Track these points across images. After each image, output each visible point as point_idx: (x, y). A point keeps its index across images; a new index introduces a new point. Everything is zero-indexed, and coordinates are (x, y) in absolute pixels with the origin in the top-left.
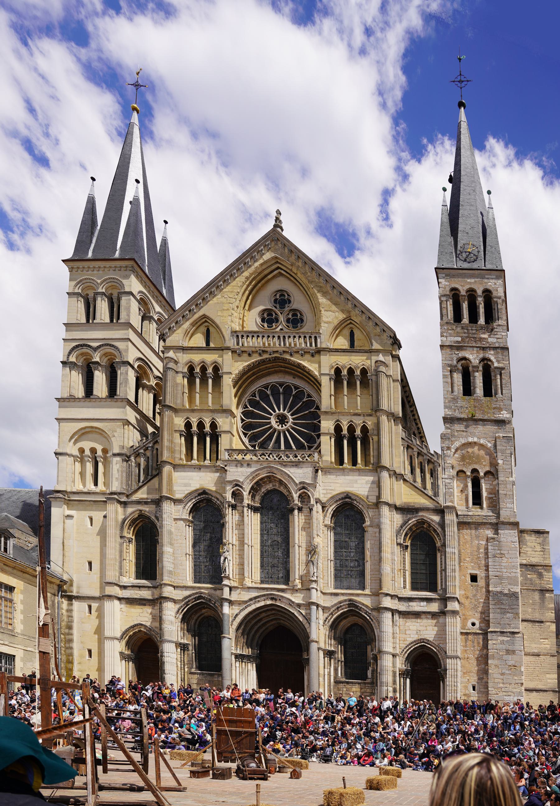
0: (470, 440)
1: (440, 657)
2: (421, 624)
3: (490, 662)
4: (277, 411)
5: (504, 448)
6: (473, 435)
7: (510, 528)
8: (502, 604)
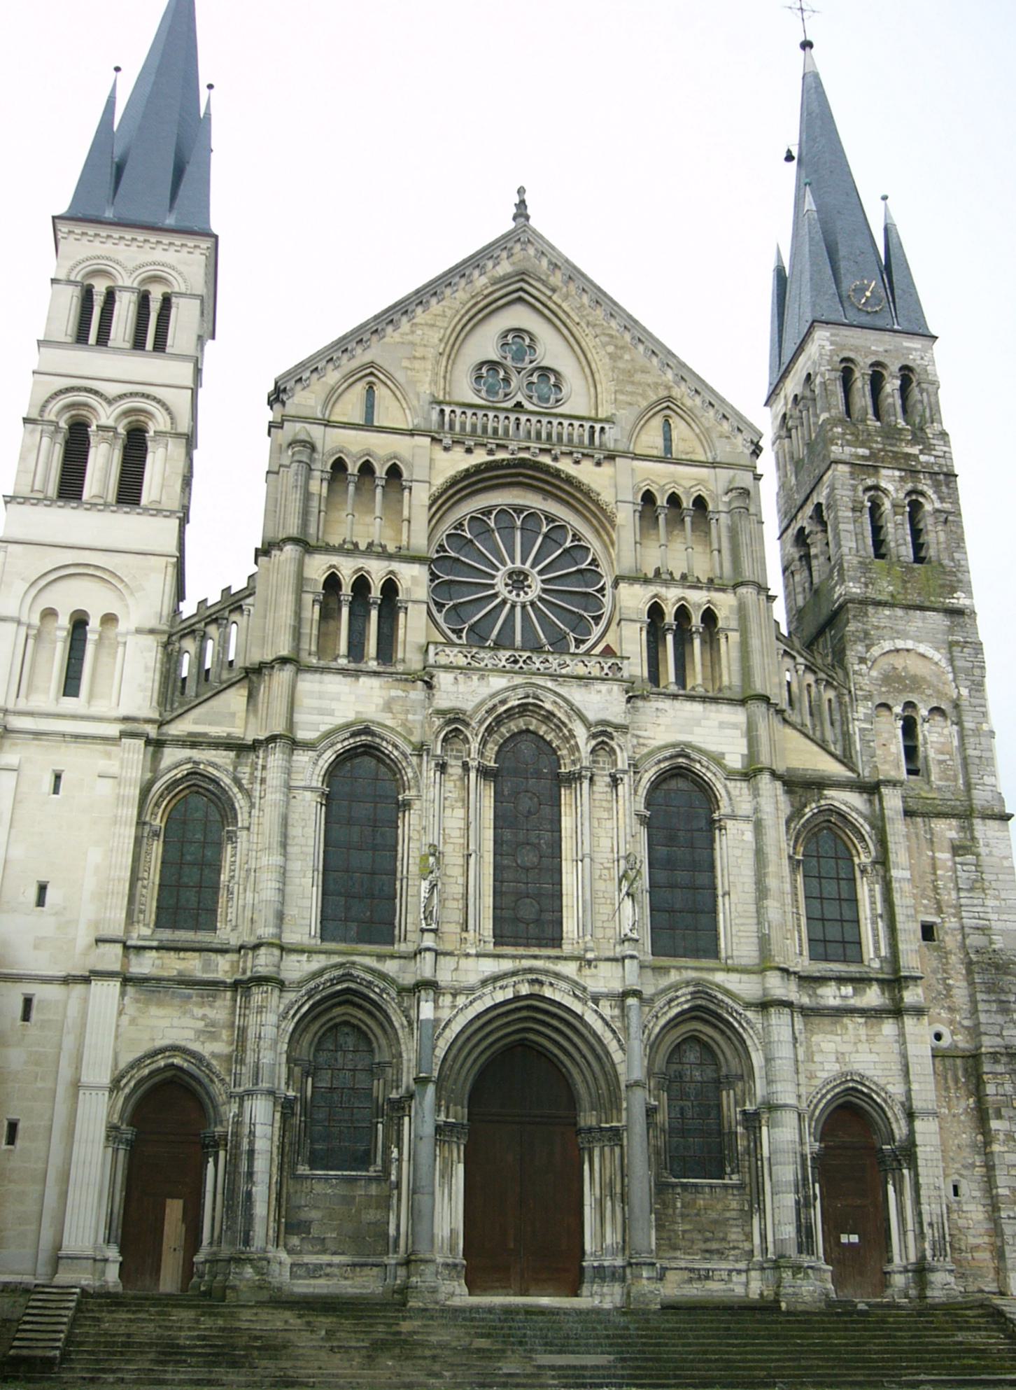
0: (900, 644)
1: (890, 1114)
2: (846, 1038)
3: (994, 1124)
5: (970, 665)
6: (903, 635)
8: (1002, 991)
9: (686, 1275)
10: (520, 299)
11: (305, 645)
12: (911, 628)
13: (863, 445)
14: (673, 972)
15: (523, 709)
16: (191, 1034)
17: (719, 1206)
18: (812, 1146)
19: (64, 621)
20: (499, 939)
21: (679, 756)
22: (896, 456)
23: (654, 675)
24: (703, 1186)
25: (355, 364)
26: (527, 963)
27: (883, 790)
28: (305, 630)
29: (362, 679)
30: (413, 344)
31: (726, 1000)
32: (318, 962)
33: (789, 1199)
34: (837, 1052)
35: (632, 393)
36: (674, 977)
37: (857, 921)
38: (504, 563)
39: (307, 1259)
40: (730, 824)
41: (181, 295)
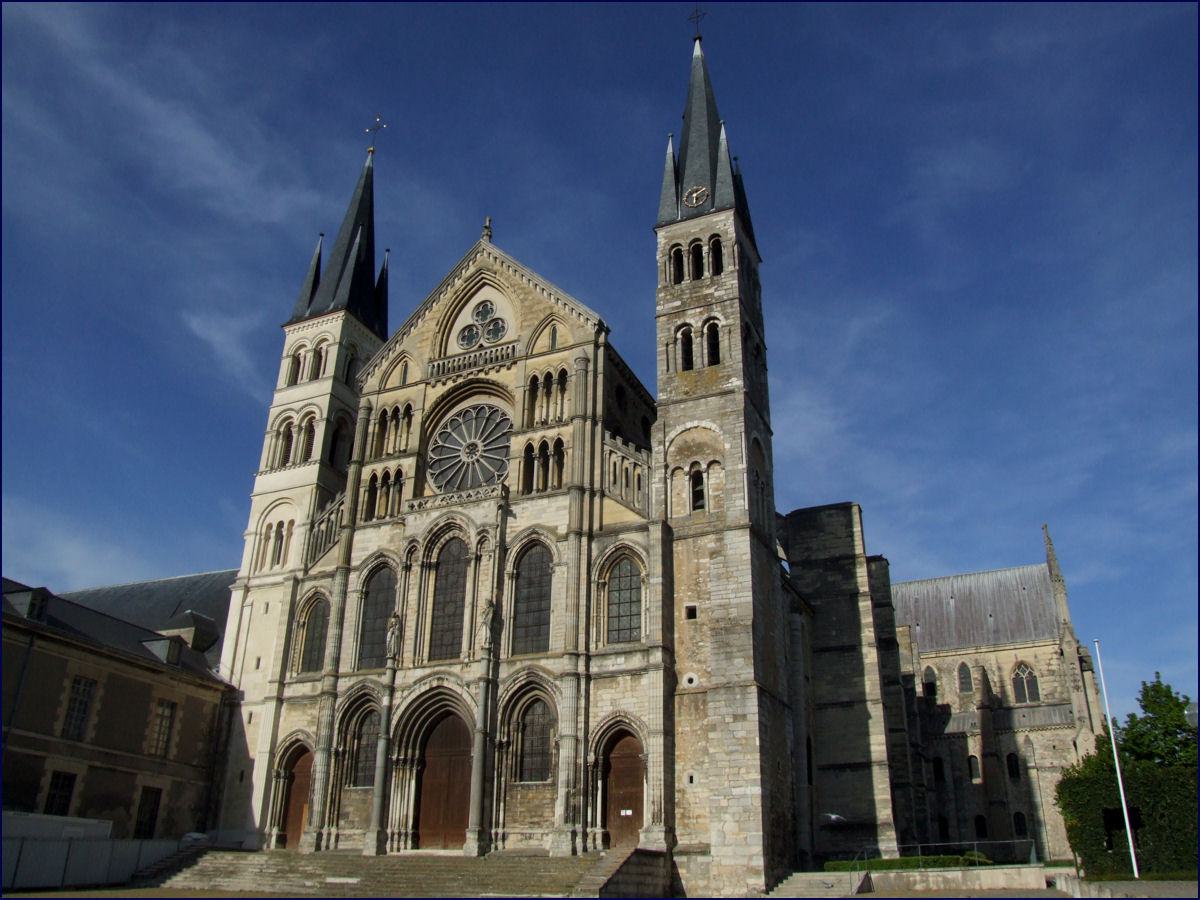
2: (618, 690)
4: (464, 444)
6: (693, 418)
7: (740, 534)
8: (728, 645)
9: (520, 837)
10: (485, 284)
11: (359, 516)
12: (698, 412)
14: (518, 663)
15: (449, 527)
16: (306, 723)
17: (540, 797)
19: (274, 528)
21: (532, 533)
22: (698, 299)
23: (528, 486)
24: (532, 786)
25: (396, 354)
26: (436, 669)
28: (360, 508)
29: (382, 527)
30: (423, 333)
31: (545, 675)
32: (354, 680)
34: (612, 699)
35: (531, 319)
36: (518, 665)
38: (465, 441)
40: (557, 569)
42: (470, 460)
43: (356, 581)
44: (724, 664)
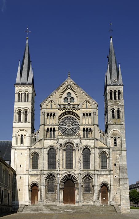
0: (114, 130)
6: (115, 128)
10: (69, 88)
11: (45, 137)
13: (112, 103)
15: (68, 142)
18: (99, 189)
19: (20, 136)
20: (66, 168)
25: (49, 100)
26: (69, 171)
27: (110, 149)
29: (52, 140)
32: (48, 172)
33: (96, 195)
36: (85, 171)
37: (107, 164)
39: (48, 201)
41: (29, 93)
42: (68, 128)
43: (46, 151)
44: (122, 174)
